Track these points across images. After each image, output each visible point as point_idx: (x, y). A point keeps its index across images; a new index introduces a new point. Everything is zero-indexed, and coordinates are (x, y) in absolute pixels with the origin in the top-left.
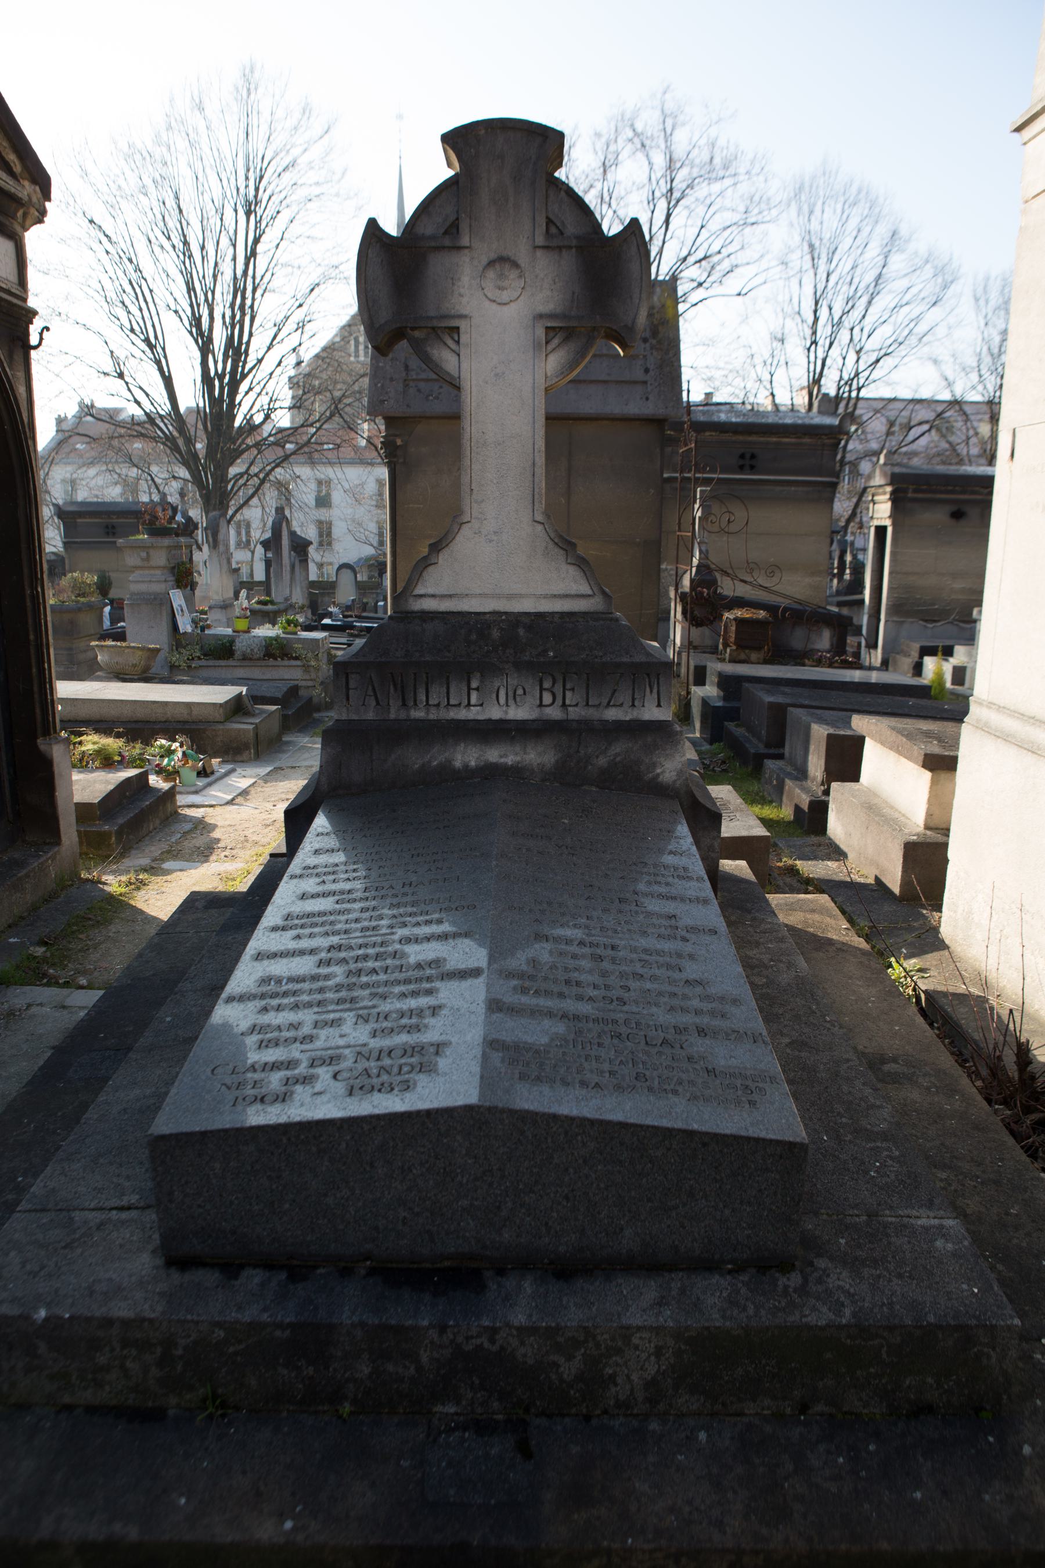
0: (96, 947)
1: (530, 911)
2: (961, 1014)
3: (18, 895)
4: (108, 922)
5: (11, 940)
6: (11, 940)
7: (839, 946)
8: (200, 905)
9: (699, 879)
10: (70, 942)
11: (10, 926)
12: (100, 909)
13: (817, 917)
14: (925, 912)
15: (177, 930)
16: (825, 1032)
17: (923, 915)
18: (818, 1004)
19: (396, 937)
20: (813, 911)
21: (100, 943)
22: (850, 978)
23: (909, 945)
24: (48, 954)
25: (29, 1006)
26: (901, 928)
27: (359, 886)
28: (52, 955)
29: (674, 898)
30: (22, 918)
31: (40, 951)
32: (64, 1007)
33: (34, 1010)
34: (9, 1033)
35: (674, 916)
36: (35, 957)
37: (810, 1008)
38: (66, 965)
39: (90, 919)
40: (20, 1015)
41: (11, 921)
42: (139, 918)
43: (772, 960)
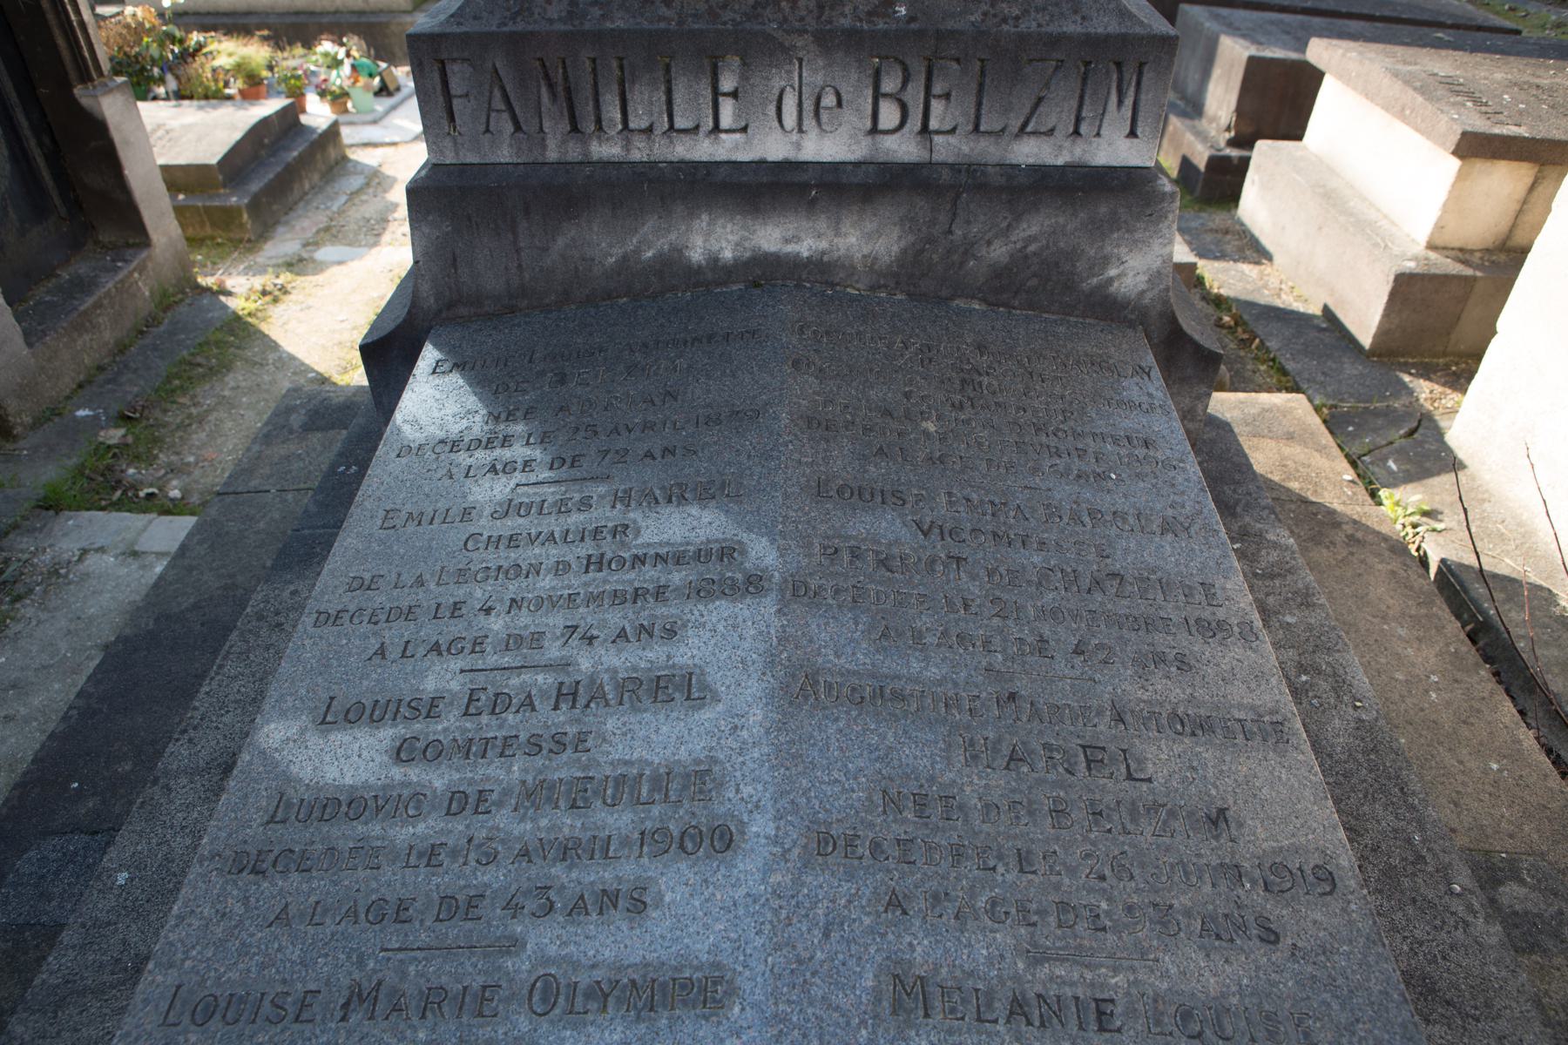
0: (201, 420)
1: (876, 847)
2: (1517, 622)
3: (87, 337)
4: (226, 367)
5: (81, 413)
6: (81, 413)
7: (1348, 529)
8: (296, 420)
9: (1247, 634)
10: (165, 411)
11: (80, 386)
12: (218, 344)
13: (1294, 451)
14: (1407, 378)
15: (253, 484)
16: (1459, 933)
17: (1404, 386)
18: (1422, 828)
19: (520, 966)
20: (1290, 437)
21: (209, 411)
22: (1384, 618)
23: (1401, 455)
24: (130, 439)
25: (84, 552)
26: (1376, 413)
27: (454, 686)
28: (137, 439)
29: (1202, 727)
30: (101, 369)
31: (114, 435)
32: (135, 554)
33: (92, 561)
34: (43, 616)
35: (1222, 811)
36: (109, 447)
37: (1409, 841)
38: (156, 457)
39: (199, 365)
40: (66, 576)
41: (82, 377)
42: (271, 357)
43: (1302, 669)
